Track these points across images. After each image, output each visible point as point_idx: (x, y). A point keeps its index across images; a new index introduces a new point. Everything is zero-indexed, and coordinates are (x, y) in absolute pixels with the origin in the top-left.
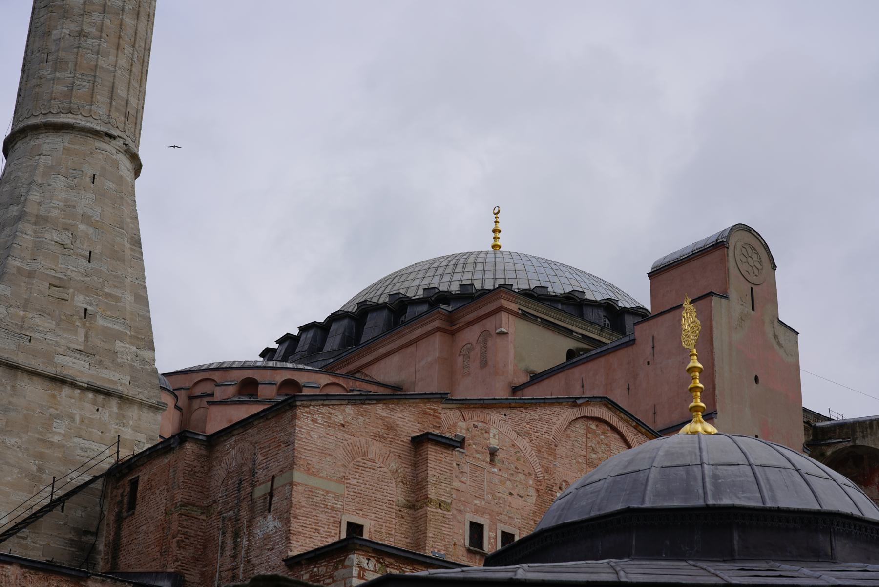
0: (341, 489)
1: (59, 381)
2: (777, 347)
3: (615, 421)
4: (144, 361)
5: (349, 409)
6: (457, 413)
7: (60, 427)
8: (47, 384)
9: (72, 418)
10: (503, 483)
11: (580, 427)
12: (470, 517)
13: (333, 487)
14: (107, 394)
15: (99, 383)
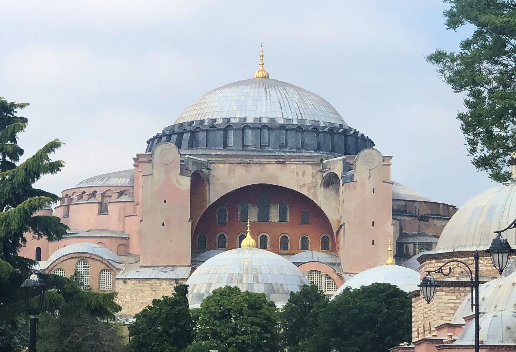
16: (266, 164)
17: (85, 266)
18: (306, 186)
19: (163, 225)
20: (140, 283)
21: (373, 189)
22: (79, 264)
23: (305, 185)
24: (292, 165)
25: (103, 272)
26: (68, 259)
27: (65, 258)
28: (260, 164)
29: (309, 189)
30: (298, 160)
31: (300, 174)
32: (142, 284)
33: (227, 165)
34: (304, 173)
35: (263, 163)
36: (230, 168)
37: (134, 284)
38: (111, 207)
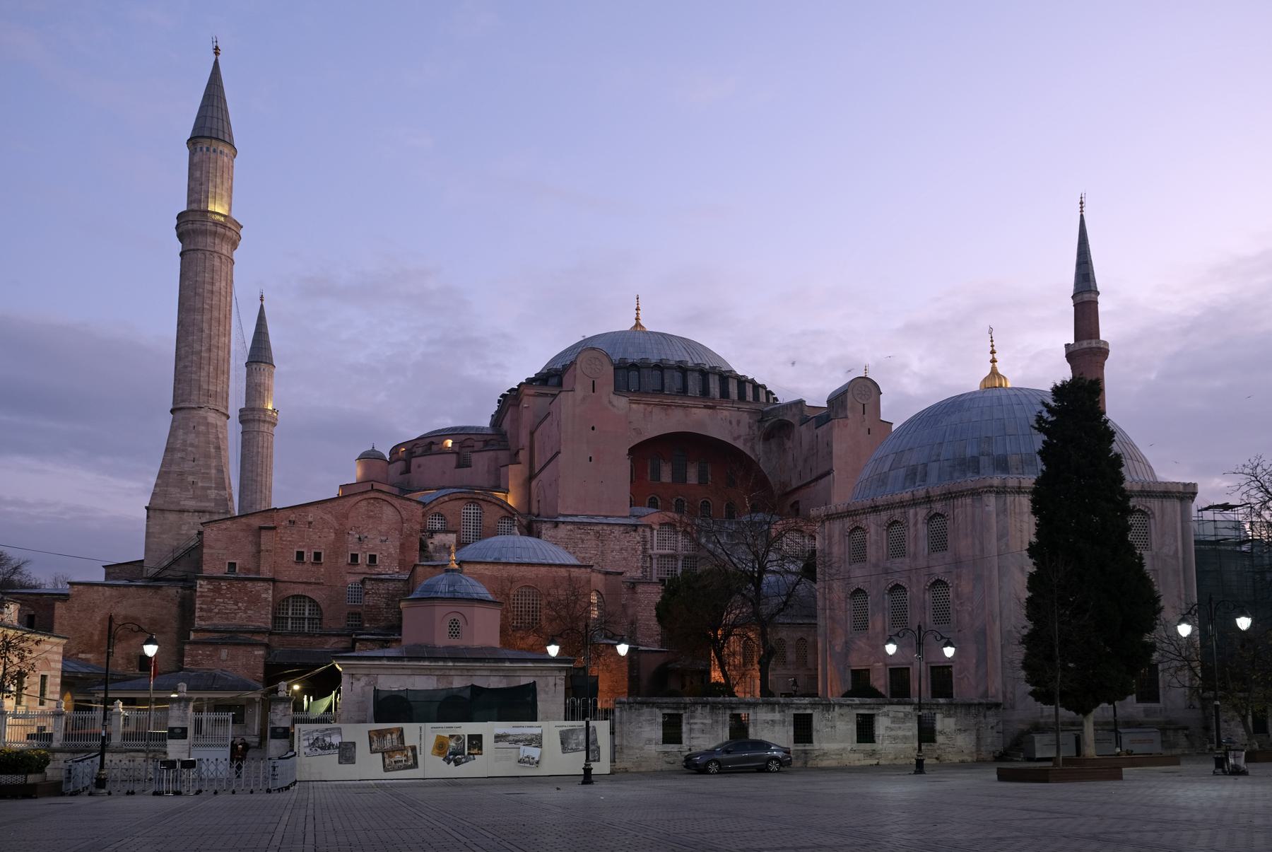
0: (225, 552)
1: (182, 511)
2: (610, 407)
3: (383, 497)
4: (221, 495)
5: (229, 523)
6: (290, 512)
7: (185, 528)
8: (178, 513)
9: (189, 523)
10: (316, 534)
11: (364, 503)
12: (296, 550)
13: (221, 551)
14: (204, 512)
15: (199, 509)
16: (691, 407)
17: (476, 511)
18: (742, 438)
19: (591, 460)
20: (580, 529)
21: (869, 429)
22: (467, 509)
23: (739, 437)
24: (724, 411)
25: (503, 521)
26: (451, 500)
27: (446, 498)
28: (685, 407)
29: (746, 441)
30: (731, 405)
31: (734, 423)
32: (582, 531)
33: (642, 405)
34: (738, 422)
35: (688, 407)
36: (645, 409)
37: (571, 530)
38: (475, 457)
